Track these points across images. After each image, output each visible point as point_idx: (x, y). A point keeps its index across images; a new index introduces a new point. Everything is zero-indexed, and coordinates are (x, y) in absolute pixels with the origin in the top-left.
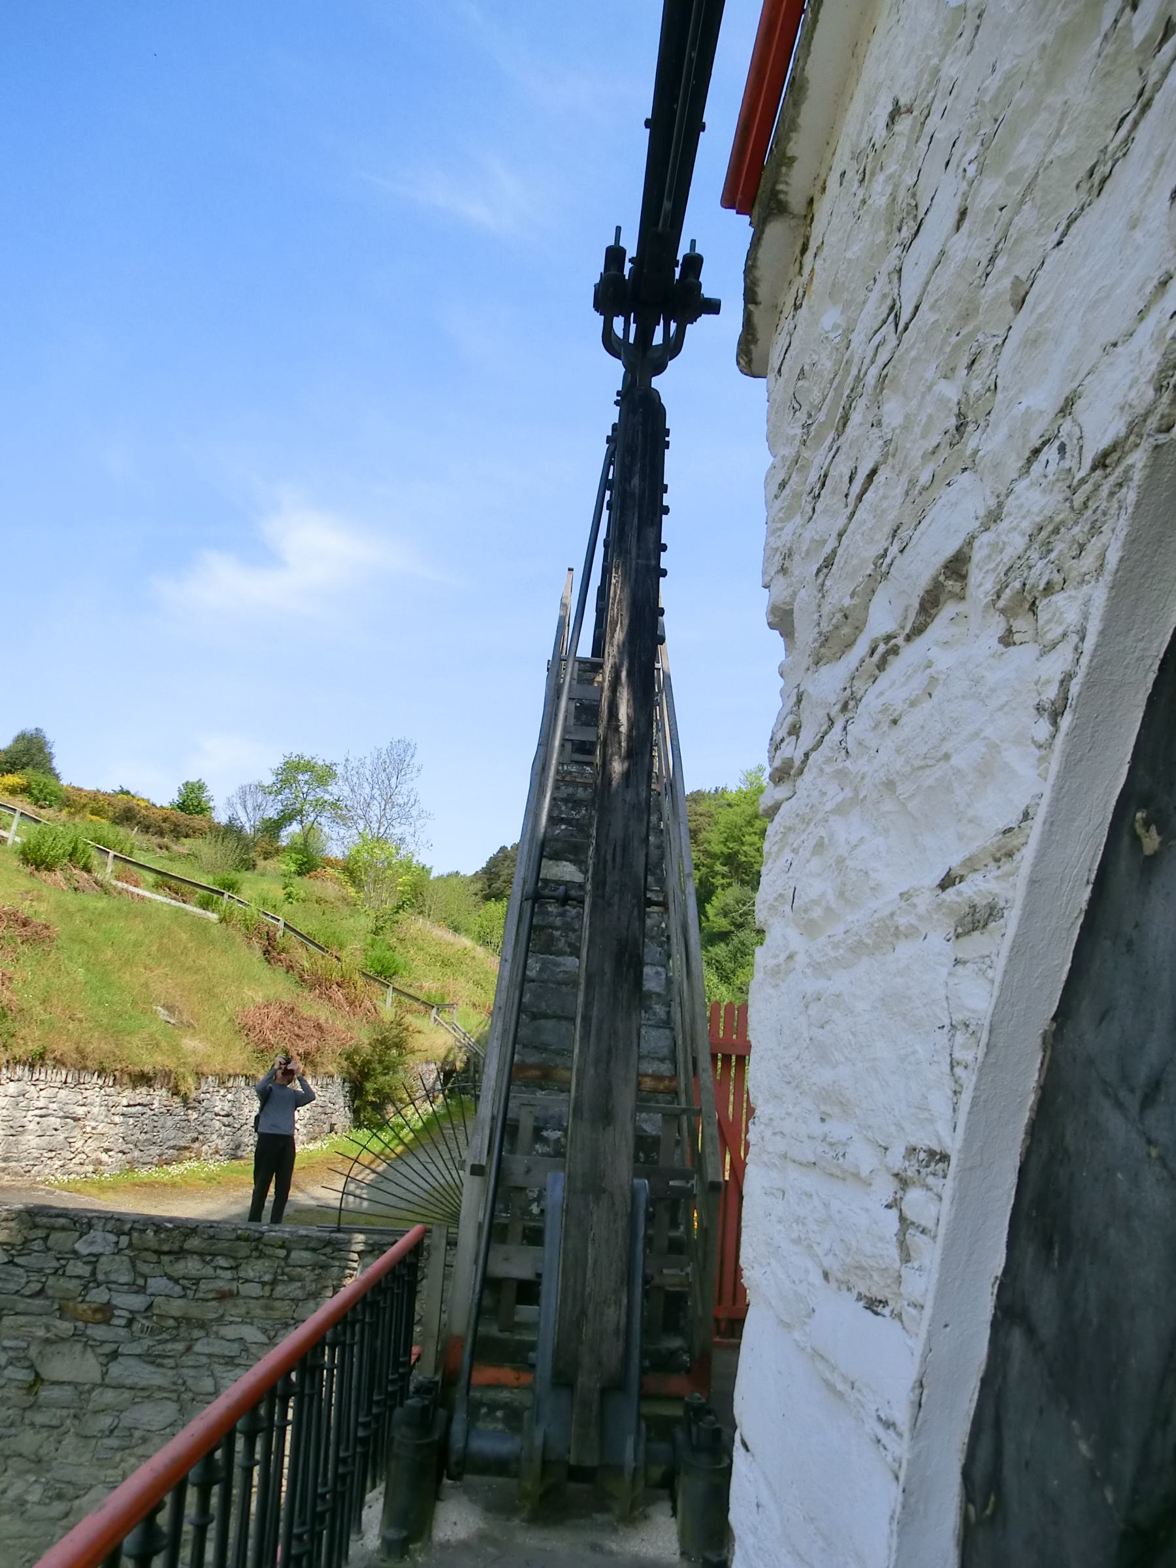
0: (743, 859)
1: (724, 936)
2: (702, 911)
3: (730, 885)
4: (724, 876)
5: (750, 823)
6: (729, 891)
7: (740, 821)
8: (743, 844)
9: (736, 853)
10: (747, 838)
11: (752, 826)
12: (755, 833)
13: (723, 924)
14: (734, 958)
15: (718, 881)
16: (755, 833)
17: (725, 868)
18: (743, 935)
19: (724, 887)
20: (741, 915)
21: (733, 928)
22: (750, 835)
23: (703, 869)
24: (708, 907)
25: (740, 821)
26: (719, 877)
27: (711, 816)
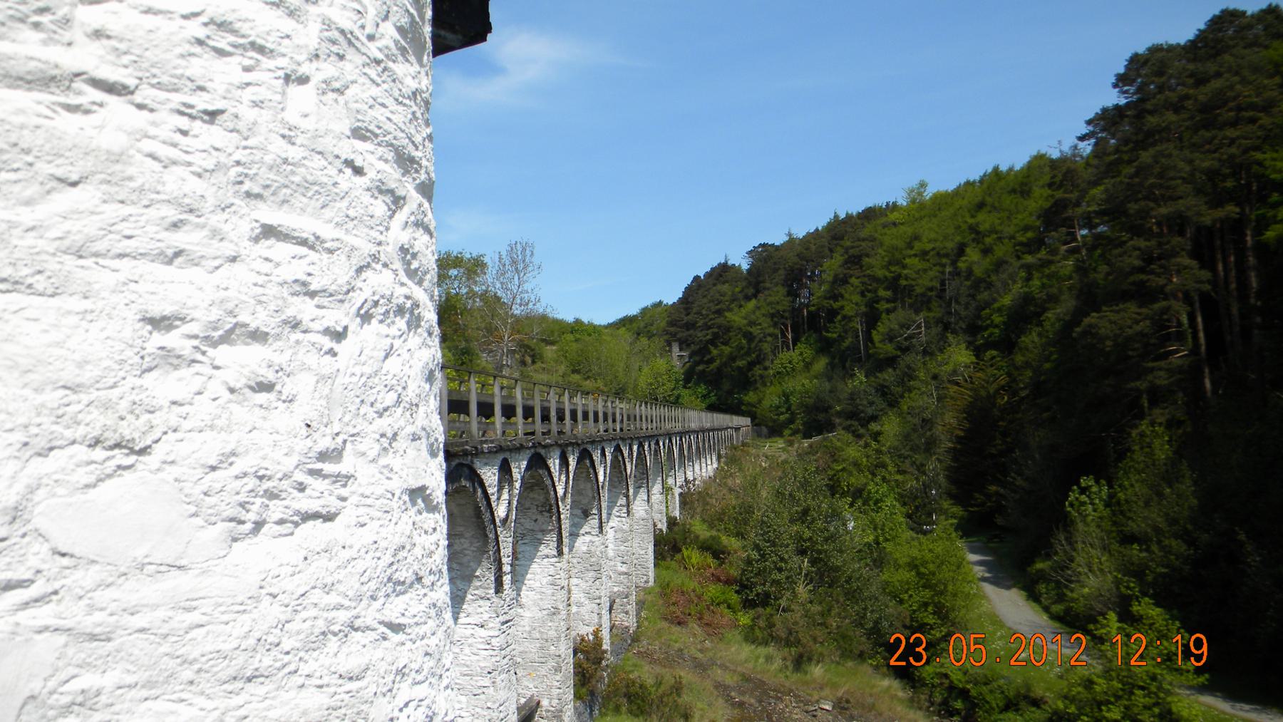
1: (891, 362)
2: (869, 338)
3: (895, 309)
4: (888, 301)
5: (910, 246)
6: (892, 316)
7: (900, 244)
8: (904, 267)
9: (899, 276)
10: (908, 261)
11: (912, 248)
12: (915, 255)
13: (889, 348)
15: (884, 306)
16: (915, 255)
17: (889, 294)
18: (908, 359)
19: (888, 311)
20: (906, 339)
22: (910, 256)
23: (869, 295)
24: (874, 332)
26: (883, 303)
27: (874, 240)
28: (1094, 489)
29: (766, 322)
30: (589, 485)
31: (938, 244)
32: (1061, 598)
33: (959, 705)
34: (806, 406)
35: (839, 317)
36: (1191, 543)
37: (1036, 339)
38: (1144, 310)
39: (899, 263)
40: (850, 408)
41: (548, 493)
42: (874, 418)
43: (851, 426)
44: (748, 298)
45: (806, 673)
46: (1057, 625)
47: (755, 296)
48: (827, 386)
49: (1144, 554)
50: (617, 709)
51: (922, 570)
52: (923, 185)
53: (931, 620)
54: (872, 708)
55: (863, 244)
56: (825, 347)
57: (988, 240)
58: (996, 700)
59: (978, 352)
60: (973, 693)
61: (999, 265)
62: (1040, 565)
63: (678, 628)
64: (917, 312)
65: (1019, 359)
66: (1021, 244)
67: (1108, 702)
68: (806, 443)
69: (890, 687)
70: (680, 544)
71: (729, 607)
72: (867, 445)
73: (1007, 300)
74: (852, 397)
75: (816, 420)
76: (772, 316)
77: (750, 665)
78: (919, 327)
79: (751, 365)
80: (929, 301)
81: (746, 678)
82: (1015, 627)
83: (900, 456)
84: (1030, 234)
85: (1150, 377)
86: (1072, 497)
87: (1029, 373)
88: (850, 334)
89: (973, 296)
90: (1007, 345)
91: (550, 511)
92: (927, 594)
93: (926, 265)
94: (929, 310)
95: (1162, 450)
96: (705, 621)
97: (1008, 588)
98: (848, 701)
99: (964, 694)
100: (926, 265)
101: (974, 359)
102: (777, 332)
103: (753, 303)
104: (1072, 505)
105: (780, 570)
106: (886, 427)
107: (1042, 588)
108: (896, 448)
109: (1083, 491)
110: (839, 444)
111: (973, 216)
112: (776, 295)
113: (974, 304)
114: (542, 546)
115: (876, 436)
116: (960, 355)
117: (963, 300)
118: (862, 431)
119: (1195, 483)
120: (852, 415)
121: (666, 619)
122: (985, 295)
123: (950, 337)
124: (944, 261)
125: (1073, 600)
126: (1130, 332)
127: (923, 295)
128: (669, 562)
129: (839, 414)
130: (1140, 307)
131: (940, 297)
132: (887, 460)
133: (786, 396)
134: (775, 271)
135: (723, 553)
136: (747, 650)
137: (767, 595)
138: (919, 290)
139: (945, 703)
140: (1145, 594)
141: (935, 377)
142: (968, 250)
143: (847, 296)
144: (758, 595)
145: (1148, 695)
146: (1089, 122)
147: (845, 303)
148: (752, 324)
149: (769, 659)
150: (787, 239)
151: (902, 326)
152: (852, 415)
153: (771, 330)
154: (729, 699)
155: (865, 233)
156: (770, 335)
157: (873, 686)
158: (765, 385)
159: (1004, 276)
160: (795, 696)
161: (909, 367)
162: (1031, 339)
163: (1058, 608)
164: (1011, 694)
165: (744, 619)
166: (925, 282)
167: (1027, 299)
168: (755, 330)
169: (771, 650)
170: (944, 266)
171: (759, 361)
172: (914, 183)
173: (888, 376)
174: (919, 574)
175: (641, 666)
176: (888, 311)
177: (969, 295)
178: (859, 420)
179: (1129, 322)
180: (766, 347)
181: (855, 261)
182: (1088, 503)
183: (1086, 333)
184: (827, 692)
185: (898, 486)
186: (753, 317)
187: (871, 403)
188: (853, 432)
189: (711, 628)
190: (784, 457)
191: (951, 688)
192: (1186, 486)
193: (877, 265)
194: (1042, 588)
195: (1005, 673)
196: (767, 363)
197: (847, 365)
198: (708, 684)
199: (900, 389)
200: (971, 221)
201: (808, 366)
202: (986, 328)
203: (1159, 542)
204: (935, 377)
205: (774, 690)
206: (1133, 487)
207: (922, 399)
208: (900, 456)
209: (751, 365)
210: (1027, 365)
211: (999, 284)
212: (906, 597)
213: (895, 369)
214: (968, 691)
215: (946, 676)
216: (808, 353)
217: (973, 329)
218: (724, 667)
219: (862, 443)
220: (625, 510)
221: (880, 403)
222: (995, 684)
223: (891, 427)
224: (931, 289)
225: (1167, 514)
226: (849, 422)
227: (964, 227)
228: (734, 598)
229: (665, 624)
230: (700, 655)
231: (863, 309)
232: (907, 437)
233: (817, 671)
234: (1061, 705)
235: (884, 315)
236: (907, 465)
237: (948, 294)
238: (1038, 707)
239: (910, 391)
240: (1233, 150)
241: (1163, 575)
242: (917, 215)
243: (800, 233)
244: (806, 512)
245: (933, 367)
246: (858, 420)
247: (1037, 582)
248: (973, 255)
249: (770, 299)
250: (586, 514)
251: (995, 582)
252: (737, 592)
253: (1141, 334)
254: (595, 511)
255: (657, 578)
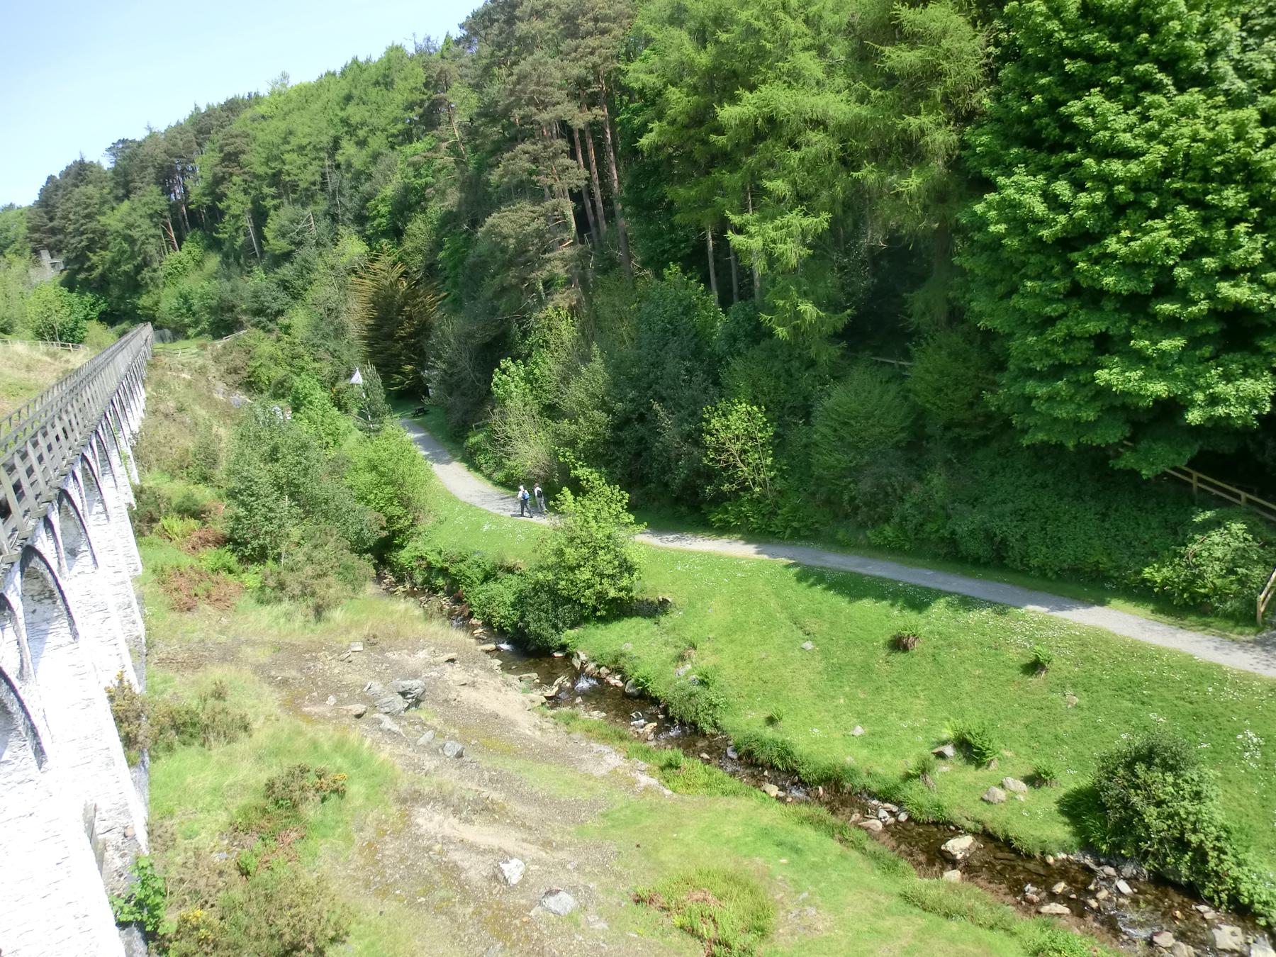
0: (288, 179)
1: (287, 256)
2: (261, 237)
4: (273, 198)
6: (281, 212)
7: (277, 140)
8: (284, 163)
9: (280, 172)
10: (286, 156)
11: (289, 143)
12: (293, 150)
13: (281, 245)
14: (301, 276)
15: (269, 203)
16: (293, 150)
17: (273, 190)
19: (276, 208)
21: (293, 247)
23: (253, 192)
24: (266, 230)
25: (277, 140)
26: (269, 199)
28: (513, 369)
29: (145, 224)
30: (71, 524)
31: (313, 139)
32: (499, 465)
33: (440, 582)
34: (210, 307)
35: (227, 217)
36: (609, 411)
37: (422, 226)
38: (537, 208)
39: (276, 158)
40: (256, 305)
41: (45, 579)
42: (280, 313)
43: (259, 322)
44: (119, 199)
45: (329, 620)
46: (502, 490)
47: (127, 196)
48: (227, 286)
49: (574, 427)
50: (170, 748)
51: (382, 469)
52: (285, 76)
53: (398, 511)
54: (397, 634)
55: (238, 140)
56: (214, 245)
57: (361, 133)
58: (476, 574)
59: (369, 240)
60: (452, 570)
61: (376, 157)
62: (473, 440)
63: (189, 615)
64: (304, 205)
65: (408, 245)
66: (393, 135)
67: (579, 566)
68: (219, 344)
69: (407, 610)
70: (156, 515)
71: (231, 572)
72: (279, 340)
73: (389, 191)
74: (256, 295)
75: (223, 323)
76: (151, 216)
77: (275, 631)
78: (308, 221)
79: (138, 269)
80: (312, 196)
81: (279, 648)
82: (468, 500)
83: (313, 345)
84: (400, 126)
85: (548, 267)
86: (496, 379)
87: (420, 257)
88: (241, 233)
89: (355, 188)
90: (396, 233)
91: (51, 595)
92: (389, 489)
93: (305, 160)
94: (316, 203)
95: (567, 331)
96: (213, 598)
97: (448, 462)
98: (375, 637)
99: (443, 572)
100: (305, 160)
101: (367, 248)
102: (160, 232)
103: (126, 202)
104: (497, 385)
105: (270, 520)
106: (295, 319)
107: (481, 459)
108: (308, 339)
109: (504, 372)
110: (252, 342)
111: (342, 109)
112: (150, 196)
113: (357, 198)
114: (50, 638)
115: (287, 329)
116: (353, 247)
117: (347, 192)
118: (271, 326)
119: (605, 361)
120: (259, 312)
121: (174, 609)
122: (366, 187)
123: (341, 230)
124: (323, 154)
125: (511, 468)
126: (528, 229)
127: (307, 189)
128: (150, 537)
129: (244, 312)
130: (534, 205)
131: (322, 190)
132: (301, 349)
133: (185, 298)
134: (144, 168)
135: (204, 512)
136: (267, 614)
137: (263, 548)
138: (303, 185)
139: (426, 581)
140: (578, 459)
141: (333, 268)
142: (344, 143)
143: (230, 194)
144: (253, 549)
145: (609, 551)
146: (461, 26)
147: (231, 202)
148: (130, 226)
149: (289, 616)
150: (147, 133)
151: (292, 222)
152: (259, 312)
153: (153, 231)
154: (271, 680)
155: (236, 127)
156: (153, 236)
157: (391, 614)
158: (157, 287)
159: (381, 167)
160: (329, 648)
161: (306, 261)
162: (419, 229)
163: (499, 476)
164: (488, 568)
165: (252, 577)
166: (308, 176)
167: (407, 190)
168: (135, 233)
169: (286, 605)
170: (322, 159)
171: (146, 263)
172: (276, 75)
173: (286, 271)
174: (378, 472)
175: (172, 679)
176: (276, 208)
177: (352, 188)
178: (264, 315)
179: (527, 221)
180: (151, 249)
181: (231, 158)
182: (509, 379)
183: (489, 233)
184: (354, 633)
185: (317, 373)
186: (130, 220)
187: (275, 299)
188: (263, 328)
189: (223, 603)
190: (200, 362)
191: (429, 567)
192: (598, 364)
193: (255, 161)
194: (481, 459)
195: (476, 548)
196: (155, 265)
197: (242, 261)
198: (247, 673)
199: (300, 282)
200: (342, 114)
201: (199, 264)
202: (374, 218)
203: (584, 414)
204: (333, 268)
205: (308, 651)
206: (548, 366)
207: (323, 290)
208: (313, 345)
209: (138, 269)
210: (418, 250)
211: (378, 176)
212: (372, 496)
213: (292, 263)
214: (447, 569)
215: (422, 558)
216: (197, 251)
217: (361, 219)
218: (247, 642)
219: (273, 337)
220: (104, 516)
221: (283, 297)
222: (470, 561)
223: (299, 319)
224: (314, 184)
225: (587, 390)
226: (257, 319)
227: (336, 120)
228: (232, 560)
229: (175, 615)
230: (223, 638)
231: (250, 206)
232: (316, 328)
233: (337, 615)
234: (540, 576)
235: (272, 212)
236: (321, 353)
237: (330, 188)
238: (514, 574)
239: (310, 283)
240: (596, 59)
241: (591, 442)
242: (286, 109)
243: (161, 126)
244: (275, 450)
245: (330, 259)
246: (266, 316)
247: (475, 453)
248: (348, 149)
249: (144, 200)
250: (73, 553)
251: (439, 461)
252: (233, 551)
253: (537, 230)
254: (84, 548)
255: (144, 560)
